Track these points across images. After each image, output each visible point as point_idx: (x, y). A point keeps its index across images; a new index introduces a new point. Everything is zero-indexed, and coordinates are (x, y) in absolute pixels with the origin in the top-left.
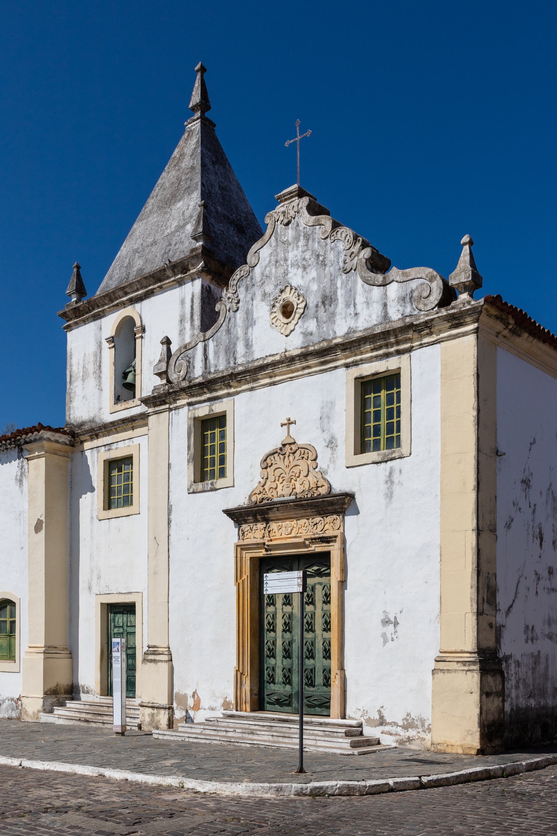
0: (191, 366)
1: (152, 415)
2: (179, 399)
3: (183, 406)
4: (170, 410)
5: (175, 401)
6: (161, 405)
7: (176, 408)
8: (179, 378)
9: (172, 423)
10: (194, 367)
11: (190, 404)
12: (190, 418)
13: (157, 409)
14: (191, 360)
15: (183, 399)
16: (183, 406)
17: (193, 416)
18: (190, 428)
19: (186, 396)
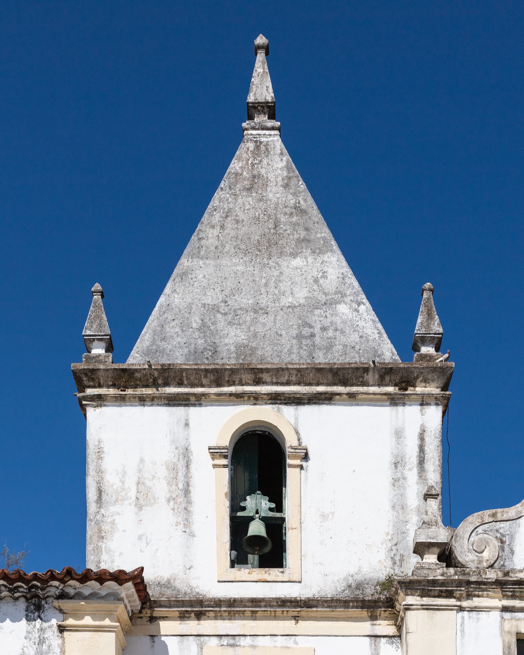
0: (507, 549)
1: (417, 609)
2: (478, 596)
3: (489, 609)
4: (461, 609)
5: (469, 596)
6: (439, 596)
7: (472, 610)
8: (480, 562)
9: (463, 631)
10: (512, 552)
11: (505, 609)
12: (509, 632)
13: (426, 601)
14: (507, 539)
15: (488, 596)
16: (489, 609)
17: (514, 630)
18: (509, 647)
19: (500, 595)
